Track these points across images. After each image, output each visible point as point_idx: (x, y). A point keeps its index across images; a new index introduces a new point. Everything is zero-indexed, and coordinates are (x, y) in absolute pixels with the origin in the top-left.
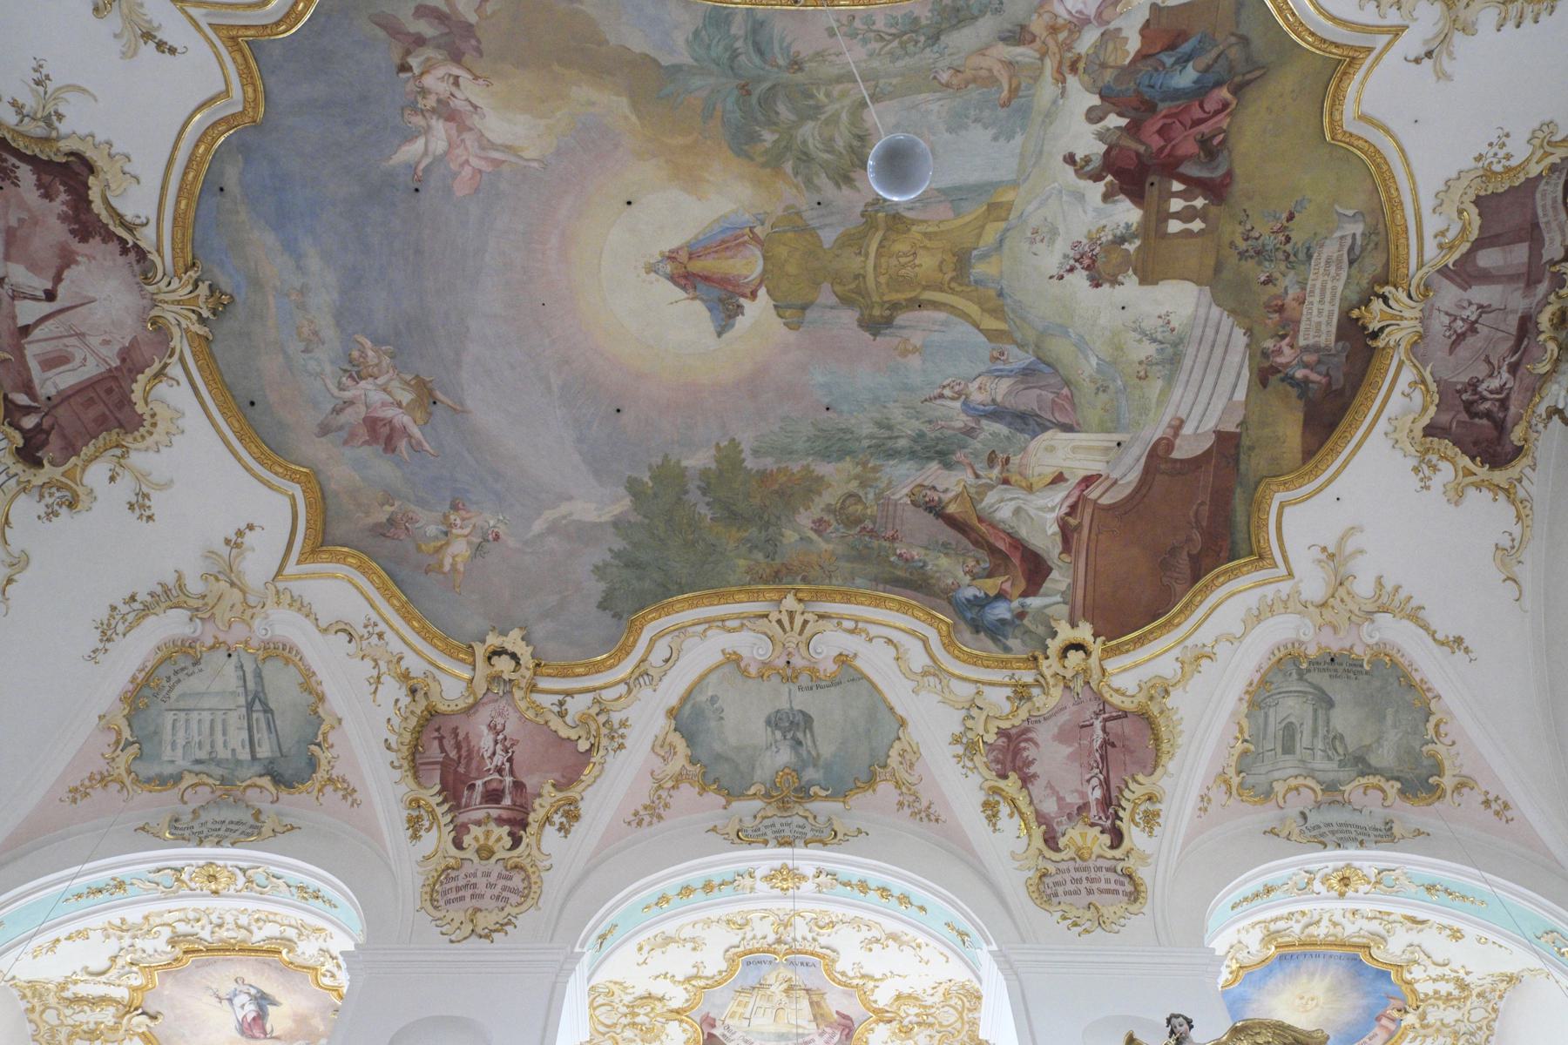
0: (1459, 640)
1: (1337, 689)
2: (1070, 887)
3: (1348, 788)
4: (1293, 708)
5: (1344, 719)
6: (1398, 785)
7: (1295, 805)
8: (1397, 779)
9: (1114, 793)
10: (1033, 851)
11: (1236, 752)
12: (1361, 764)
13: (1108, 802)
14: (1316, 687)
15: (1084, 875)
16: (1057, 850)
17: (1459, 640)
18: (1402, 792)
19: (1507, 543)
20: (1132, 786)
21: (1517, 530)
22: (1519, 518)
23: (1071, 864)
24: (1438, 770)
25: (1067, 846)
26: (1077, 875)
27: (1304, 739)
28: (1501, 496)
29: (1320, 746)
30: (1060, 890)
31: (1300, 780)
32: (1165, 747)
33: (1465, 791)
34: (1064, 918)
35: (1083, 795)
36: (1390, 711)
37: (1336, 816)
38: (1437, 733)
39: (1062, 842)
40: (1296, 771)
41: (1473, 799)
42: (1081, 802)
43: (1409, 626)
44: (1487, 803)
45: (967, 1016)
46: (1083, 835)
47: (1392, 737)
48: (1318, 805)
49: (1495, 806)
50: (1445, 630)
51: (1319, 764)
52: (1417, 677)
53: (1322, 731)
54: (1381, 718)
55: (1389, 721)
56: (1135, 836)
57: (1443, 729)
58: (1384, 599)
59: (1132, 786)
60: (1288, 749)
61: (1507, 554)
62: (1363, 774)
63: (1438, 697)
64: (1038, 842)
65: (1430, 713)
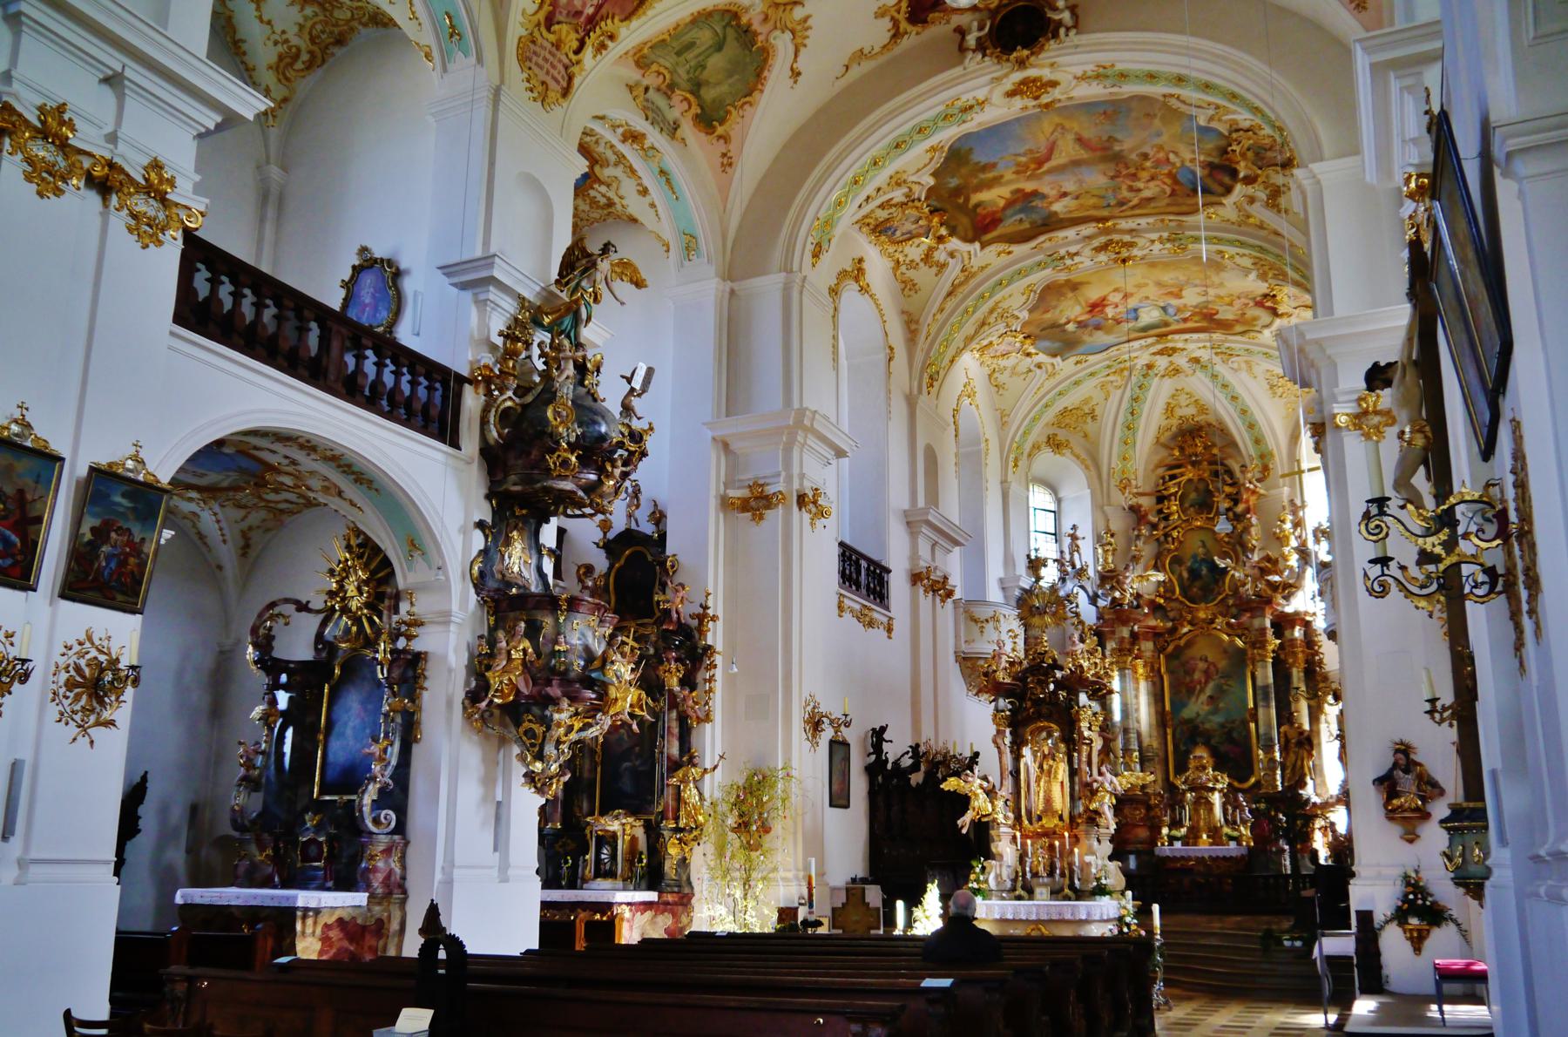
0: (799, 74)
1: (732, 48)
2: (540, 61)
3: (678, 92)
4: (705, 37)
5: (716, 62)
6: (699, 111)
7: (651, 80)
8: (702, 108)
9: (598, 18)
10: (535, 19)
11: (661, 38)
12: (696, 87)
13: (592, 22)
14: (725, 38)
15: (551, 59)
16: (549, 29)
17: (799, 74)
18: (697, 116)
19: (865, 52)
20: (609, 21)
21: (877, 49)
22: (884, 47)
23: (548, 46)
24: (722, 122)
25: (554, 33)
26: (548, 56)
27: (690, 55)
28: (892, 32)
29: (692, 64)
30: (535, 58)
31: (666, 72)
32: (641, 11)
33: (722, 141)
34: (528, 81)
35: (584, 5)
36: (737, 77)
37: (660, 101)
38: (742, 106)
39: (555, 28)
40: (668, 65)
41: (721, 147)
42: (580, 8)
43: (791, 49)
44: (724, 155)
45: (355, 24)
46: (568, 33)
47: (724, 88)
48: (658, 89)
49: (725, 160)
50: (799, 66)
51: (682, 71)
52: (766, 73)
53: (700, 58)
54: (730, 75)
55: (730, 81)
56: (588, 51)
57: (746, 107)
58: (799, 28)
59: (609, 21)
60: (679, 54)
61: (861, 55)
62: (692, 92)
63: (762, 91)
64: (541, 16)
65: (750, 94)
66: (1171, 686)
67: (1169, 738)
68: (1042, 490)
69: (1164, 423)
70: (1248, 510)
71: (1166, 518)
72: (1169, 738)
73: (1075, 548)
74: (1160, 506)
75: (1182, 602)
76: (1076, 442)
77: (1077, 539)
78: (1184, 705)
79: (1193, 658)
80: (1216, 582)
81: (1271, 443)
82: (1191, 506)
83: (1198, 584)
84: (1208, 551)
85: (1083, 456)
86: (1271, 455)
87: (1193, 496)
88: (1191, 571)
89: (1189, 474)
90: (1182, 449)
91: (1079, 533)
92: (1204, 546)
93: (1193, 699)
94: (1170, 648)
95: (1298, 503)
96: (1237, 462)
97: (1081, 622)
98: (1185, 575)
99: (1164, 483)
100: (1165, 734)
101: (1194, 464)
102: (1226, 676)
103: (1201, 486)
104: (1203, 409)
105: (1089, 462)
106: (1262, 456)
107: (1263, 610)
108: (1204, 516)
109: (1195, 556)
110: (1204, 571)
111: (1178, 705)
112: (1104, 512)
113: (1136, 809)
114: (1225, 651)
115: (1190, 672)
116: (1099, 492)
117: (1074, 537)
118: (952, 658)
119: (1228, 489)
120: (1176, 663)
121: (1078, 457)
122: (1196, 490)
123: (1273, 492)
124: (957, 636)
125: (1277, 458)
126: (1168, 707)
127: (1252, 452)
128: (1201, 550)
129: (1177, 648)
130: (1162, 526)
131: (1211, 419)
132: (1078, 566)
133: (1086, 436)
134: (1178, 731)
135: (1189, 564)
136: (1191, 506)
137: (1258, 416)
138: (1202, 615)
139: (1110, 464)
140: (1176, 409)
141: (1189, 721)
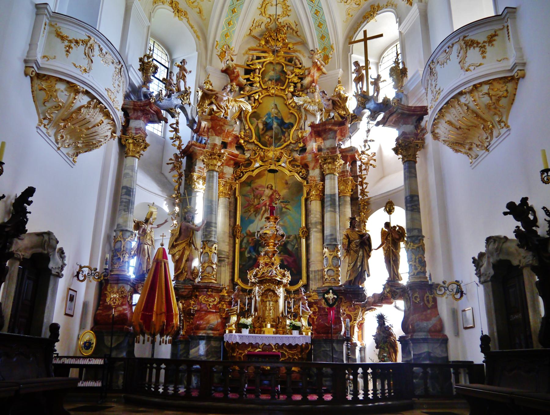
66: (243, 207)
67: (237, 246)
68: (160, 48)
69: (258, 18)
70: (313, 81)
71: (251, 85)
72: (237, 246)
73: (182, 77)
74: (247, 76)
75: (256, 145)
76: (193, 14)
77: (185, 70)
78: (252, 222)
79: (261, 186)
80: (283, 133)
81: (332, 40)
82: (270, 80)
83: (269, 133)
84: (279, 112)
85: (196, 28)
86: (332, 47)
87: (272, 73)
88: (266, 124)
89: (270, 58)
90: (267, 42)
91: (186, 67)
92: (277, 108)
93: (259, 217)
94: (244, 178)
95: (362, 64)
96: (304, 56)
97: (178, 138)
98: (261, 126)
99: (252, 60)
100: (235, 243)
101: (273, 52)
102: (285, 201)
103: (278, 68)
104: (287, 11)
105: (199, 34)
106: (324, 49)
107: (335, 132)
108: (279, 88)
109: (269, 115)
110: (275, 125)
111: (246, 221)
112: (206, 71)
113: (210, 296)
114: (287, 183)
115: (259, 196)
116: (204, 57)
117: (182, 68)
118: (19, 67)
119: (297, 71)
120: (248, 188)
121: (192, 28)
122: (274, 70)
123: (331, 72)
124: (32, 45)
125: (335, 51)
126: (238, 222)
127: (317, 46)
128: (274, 111)
129: (250, 177)
130: (248, 88)
131: (290, 20)
132: (183, 89)
133: (200, 12)
134: (245, 241)
135: (264, 119)
136: (270, 80)
137: (327, 18)
138: (271, 154)
139: (215, 38)
140: (269, 6)
141: (253, 234)
